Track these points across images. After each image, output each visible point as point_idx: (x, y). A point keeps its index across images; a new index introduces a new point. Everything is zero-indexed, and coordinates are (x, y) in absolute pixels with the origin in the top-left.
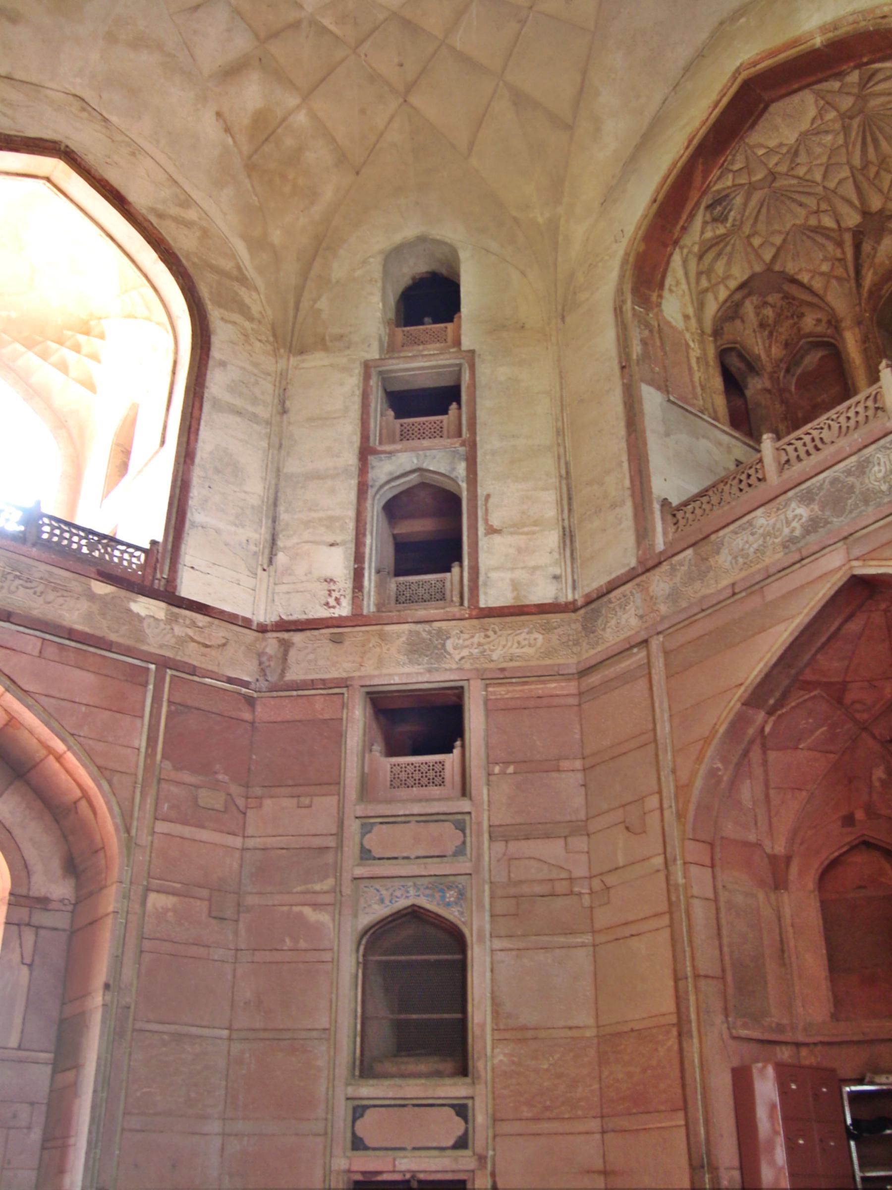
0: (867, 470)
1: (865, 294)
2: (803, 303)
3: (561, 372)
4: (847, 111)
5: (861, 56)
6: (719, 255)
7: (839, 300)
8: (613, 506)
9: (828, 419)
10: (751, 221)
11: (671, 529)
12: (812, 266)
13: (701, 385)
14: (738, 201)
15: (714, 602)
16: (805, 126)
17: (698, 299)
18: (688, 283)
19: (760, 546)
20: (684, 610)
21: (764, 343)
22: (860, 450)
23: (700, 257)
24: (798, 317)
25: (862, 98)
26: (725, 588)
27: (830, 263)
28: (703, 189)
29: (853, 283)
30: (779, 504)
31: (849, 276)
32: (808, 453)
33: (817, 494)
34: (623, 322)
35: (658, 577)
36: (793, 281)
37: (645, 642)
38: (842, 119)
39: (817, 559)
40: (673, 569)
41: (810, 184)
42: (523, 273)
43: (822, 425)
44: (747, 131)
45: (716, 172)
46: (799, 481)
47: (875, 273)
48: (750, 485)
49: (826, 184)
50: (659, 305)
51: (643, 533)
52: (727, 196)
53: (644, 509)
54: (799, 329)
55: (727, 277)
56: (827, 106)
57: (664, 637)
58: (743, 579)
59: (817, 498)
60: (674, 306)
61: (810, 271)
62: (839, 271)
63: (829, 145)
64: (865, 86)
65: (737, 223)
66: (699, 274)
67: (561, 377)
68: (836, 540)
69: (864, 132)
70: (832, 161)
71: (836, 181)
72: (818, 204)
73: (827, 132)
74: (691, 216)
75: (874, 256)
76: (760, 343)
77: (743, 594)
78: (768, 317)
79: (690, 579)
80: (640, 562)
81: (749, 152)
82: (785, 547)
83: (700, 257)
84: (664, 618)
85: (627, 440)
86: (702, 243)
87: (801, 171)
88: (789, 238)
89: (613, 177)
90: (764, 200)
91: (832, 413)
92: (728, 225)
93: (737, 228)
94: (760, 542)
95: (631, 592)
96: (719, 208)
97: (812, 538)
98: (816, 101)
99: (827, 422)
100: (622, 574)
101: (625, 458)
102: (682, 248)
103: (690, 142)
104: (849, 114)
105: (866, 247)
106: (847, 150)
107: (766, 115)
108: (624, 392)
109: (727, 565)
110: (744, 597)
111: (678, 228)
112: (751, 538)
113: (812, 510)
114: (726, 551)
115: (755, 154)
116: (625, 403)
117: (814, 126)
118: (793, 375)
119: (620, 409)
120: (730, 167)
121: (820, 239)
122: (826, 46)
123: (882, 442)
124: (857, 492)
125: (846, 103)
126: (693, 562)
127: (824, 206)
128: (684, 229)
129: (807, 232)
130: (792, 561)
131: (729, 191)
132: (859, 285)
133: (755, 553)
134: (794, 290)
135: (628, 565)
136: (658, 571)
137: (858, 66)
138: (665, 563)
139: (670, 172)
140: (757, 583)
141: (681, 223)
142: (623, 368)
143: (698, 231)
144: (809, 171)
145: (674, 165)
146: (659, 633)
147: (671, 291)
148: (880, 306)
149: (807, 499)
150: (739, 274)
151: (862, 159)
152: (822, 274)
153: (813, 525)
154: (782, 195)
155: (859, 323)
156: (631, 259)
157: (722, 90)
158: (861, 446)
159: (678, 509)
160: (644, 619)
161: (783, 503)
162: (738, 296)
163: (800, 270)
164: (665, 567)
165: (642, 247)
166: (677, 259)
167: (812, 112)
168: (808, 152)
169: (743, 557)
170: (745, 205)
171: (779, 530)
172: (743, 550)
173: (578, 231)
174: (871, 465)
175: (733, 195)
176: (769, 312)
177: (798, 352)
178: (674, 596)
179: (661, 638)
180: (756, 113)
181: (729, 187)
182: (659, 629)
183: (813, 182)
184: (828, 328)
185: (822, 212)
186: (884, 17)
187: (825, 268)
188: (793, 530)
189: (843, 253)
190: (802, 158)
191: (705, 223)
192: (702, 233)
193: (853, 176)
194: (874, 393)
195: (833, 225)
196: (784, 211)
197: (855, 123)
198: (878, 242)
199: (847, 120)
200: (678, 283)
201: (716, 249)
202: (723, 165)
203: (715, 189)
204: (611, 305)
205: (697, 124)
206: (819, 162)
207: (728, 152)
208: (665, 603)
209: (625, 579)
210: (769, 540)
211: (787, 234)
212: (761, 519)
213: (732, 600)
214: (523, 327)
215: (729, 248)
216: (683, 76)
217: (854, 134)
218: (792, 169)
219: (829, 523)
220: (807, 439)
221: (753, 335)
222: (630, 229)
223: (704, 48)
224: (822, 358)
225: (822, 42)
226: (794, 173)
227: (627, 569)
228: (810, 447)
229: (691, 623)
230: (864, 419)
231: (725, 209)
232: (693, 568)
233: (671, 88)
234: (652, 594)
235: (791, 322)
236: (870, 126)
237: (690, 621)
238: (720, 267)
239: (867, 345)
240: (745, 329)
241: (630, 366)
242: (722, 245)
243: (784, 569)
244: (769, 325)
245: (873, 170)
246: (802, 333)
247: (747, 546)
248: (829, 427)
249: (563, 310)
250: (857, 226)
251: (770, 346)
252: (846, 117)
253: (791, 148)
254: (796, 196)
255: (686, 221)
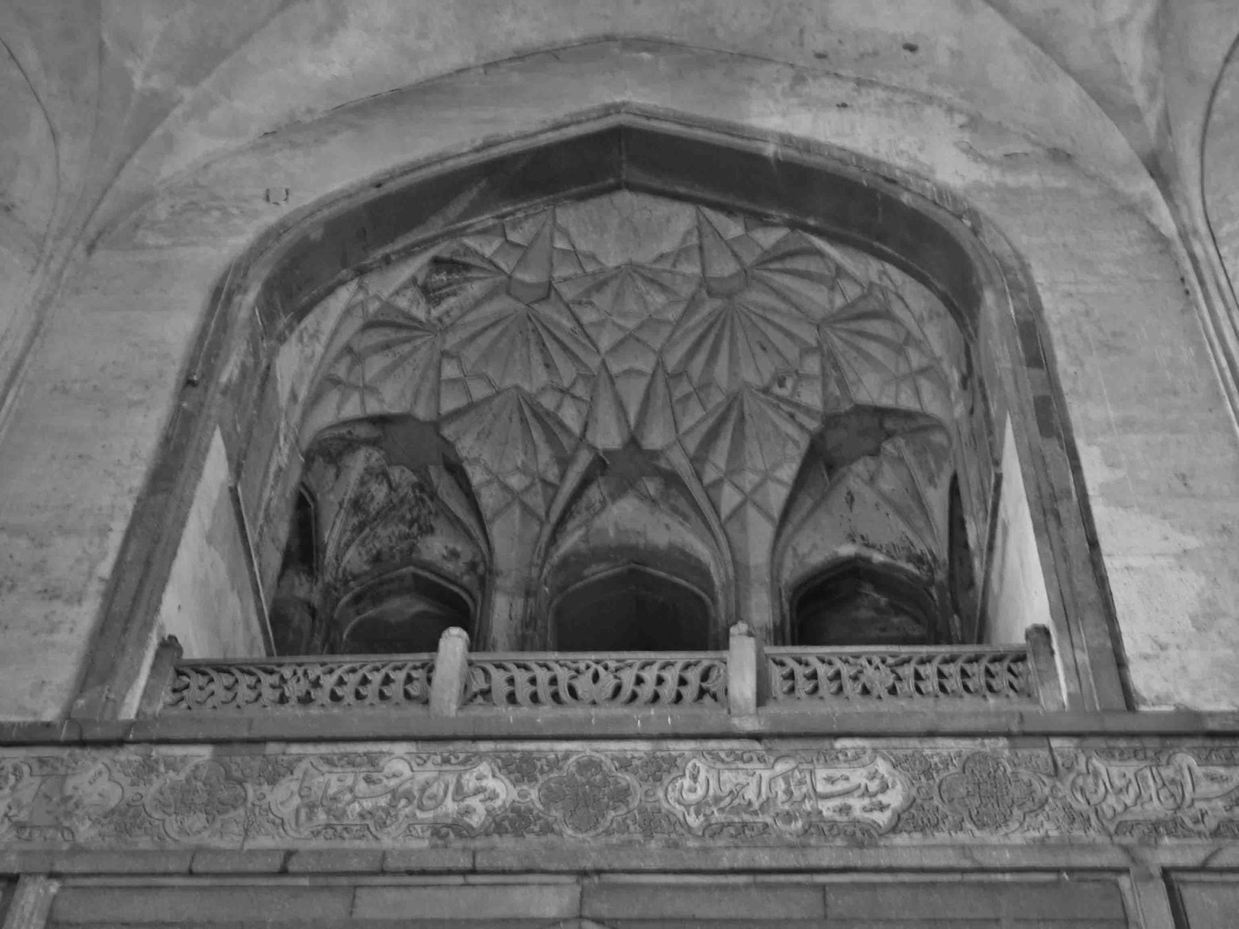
0: (667, 779)
1: (556, 557)
2: (445, 511)
3: (39, 323)
4: (721, 280)
5: (809, 214)
6: (387, 346)
7: (509, 543)
8: (50, 594)
9: (597, 662)
10: (463, 334)
11: (167, 696)
12: (498, 464)
13: (267, 510)
14: (475, 289)
15: (229, 868)
16: (644, 256)
17: (320, 383)
18: (328, 347)
19: (378, 808)
20: (144, 854)
21: (344, 531)
22: (663, 737)
23: (370, 325)
24: (420, 528)
25: (747, 277)
26: (268, 852)
27: (527, 481)
28: (453, 227)
29: (547, 530)
30: (452, 753)
31: (547, 514)
32: (535, 698)
33: (542, 772)
34: (224, 315)
35: (100, 766)
36: (456, 470)
37: (12, 880)
38: (701, 285)
39: (505, 885)
40: (149, 767)
41: (585, 341)
42: (54, 135)
43: (582, 666)
44: (567, 198)
45: (487, 219)
46: (513, 731)
47: (585, 539)
48: (382, 696)
49: (609, 361)
50: (282, 339)
51: (99, 666)
52: (467, 267)
53: (125, 630)
54: (412, 548)
55: (369, 389)
56: (696, 254)
57: (62, 888)
58: (319, 853)
59: (541, 779)
60: (292, 364)
61: (489, 472)
62: (536, 501)
63: (652, 309)
64: (764, 262)
65: (447, 321)
66: (348, 349)
67: (36, 332)
68: (564, 867)
69: (711, 326)
70: (640, 335)
71: (626, 367)
72: (574, 384)
73: (663, 288)
74: (408, 253)
75: (597, 514)
76: (336, 529)
77: (305, 882)
78: (373, 498)
79: (182, 800)
80: (68, 716)
81: (547, 230)
82: (436, 833)
83: (370, 325)
84: (77, 850)
85: (139, 500)
86: (387, 306)
87: (588, 316)
88: (496, 401)
89: (310, 111)
90: (507, 317)
91: (611, 658)
92: (435, 313)
93: (441, 328)
94: (383, 802)
95: (16, 770)
96: (443, 277)
97: (507, 843)
98: (689, 233)
99: (594, 666)
100: (13, 725)
101: (119, 527)
102: (361, 287)
103: (487, 145)
104: (712, 284)
105: (594, 494)
106: (673, 333)
107: (605, 200)
108: (172, 423)
109: (287, 812)
110: (304, 887)
111: (379, 254)
112: (362, 786)
113: (523, 795)
114: (295, 786)
115: (552, 240)
116: (166, 440)
117: (658, 266)
118: (358, 613)
119: (149, 443)
120: (508, 231)
121: (537, 434)
122: (778, 161)
123: (712, 744)
124: (634, 804)
125: (724, 267)
126: (203, 773)
127: (580, 390)
128: (387, 260)
129: (527, 413)
130: (450, 865)
131: (476, 261)
132: (553, 540)
133: (362, 816)
134: (443, 483)
135: (35, 714)
136: (106, 755)
137: (793, 225)
138: (132, 748)
139: (429, 163)
140: (347, 874)
141: (388, 249)
142: (190, 383)
143: (394, 285)
144: (600, 324)
145: (442, 158)
146: (52, 875)
147: (301, 339)
148: (570, 589)
149: (521, 770)
150: (391, 398)
151: (680, 362)
152: (505, 487)
153: (515, 821)
154: (535, 330)
155: (529, 593)
156: (287, 238)
157: (579, 114)
158: (668, 731)
159: (198, 668)
160: (26, 834)
161: (462, 756)
162: (363, 431)
163: (476, 461)
164: (130, 755)
165: (316, 235)
166: (344, 295)
167: (668, 245)
168: (618, 296)
169: (328, 812)
170: (478, 303)
171: (433, 797)
172: (334, 799)
173: (194, 147)
174: (675, 773)
175: (474, 274)
176: (380, 492)
177: (392, 580)
178: (125, 818)
179: (54, 887)
180: (600, 184)
181: (483, 257)
182: (58, 867)
183: (595, 345)
184: (468, 572)
185: (573, 397)
186: (893, 182)
187: (516, 482)
188: (468, 811)
189: (562, 476)
190: (603, 300)
191: (414, 280)
192: (397, 293)
193: (654, 375)
194: (706, 663)
195: (576, 428)
196: (517, 355)
197: (710, 306)
198: (615, 497)
199: (704, 294)
200: (315, 336)
201: (390, 334)
202: (503, 216)
203: (470, 242)
204: (211, 279)
205: (511, 130)
206: (621, 322)
207: (520, 205)
208: (95, 822)
209: (14, 735)
210: (404, 809)
211: (498, 393)
212: (398, 762)
213: (272, 882)
214: (7, 209)
215: (407, 348)
216: (510, 59)
217: (698, 317)
218: (580, 303)
219: (552, 831)
220: (543, 676)
221: (336, 508)
222: (306, 198)
223: (564, 49)
224: (421, 615)
225: (776, 153)
226: (576, 309)
227: (30, 719)
228: (544, 691)
229: (149, 887)
230: (674, 695)
231: (450, 284)
232: (199, 784)
233: (482, 62)
234: (69, 791)
235: (404, 528)
236: (723, 325)
237: (147, 880)
238: (376, 364)
239: (530, 632)
240: (332, 489)
241: (206, 389)
242: (404, 334)
243: (423, 873)
244: (367, 513)
245: (684, 388)
246: (414, 555)
247: (348, 797)
248: (596, 677)
249: (100, 234)
250: (606, 452)
251: (348, 546)
252: (706, 285)
253: (602, 271)
254: (551, 346)
255: (397, 252)
